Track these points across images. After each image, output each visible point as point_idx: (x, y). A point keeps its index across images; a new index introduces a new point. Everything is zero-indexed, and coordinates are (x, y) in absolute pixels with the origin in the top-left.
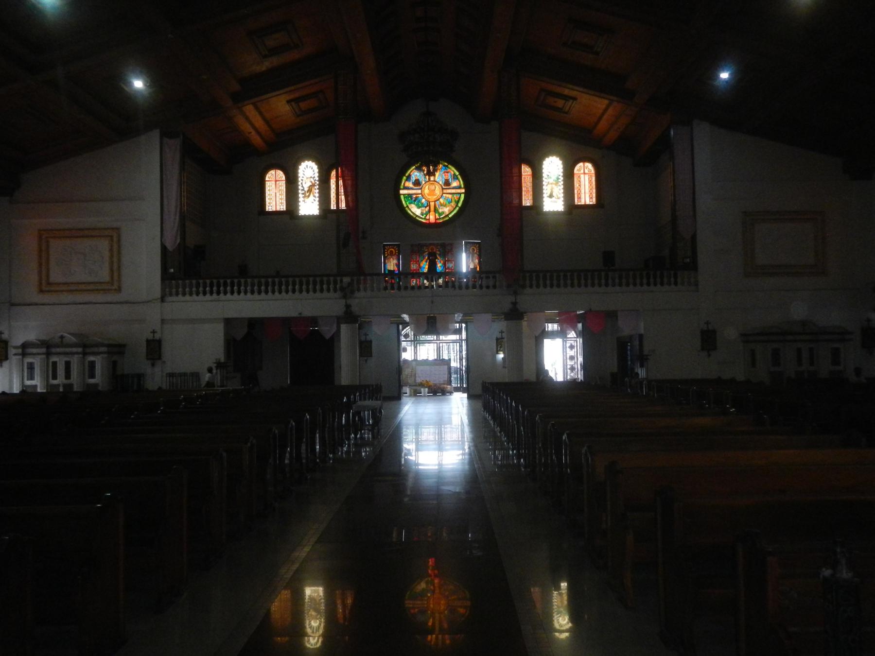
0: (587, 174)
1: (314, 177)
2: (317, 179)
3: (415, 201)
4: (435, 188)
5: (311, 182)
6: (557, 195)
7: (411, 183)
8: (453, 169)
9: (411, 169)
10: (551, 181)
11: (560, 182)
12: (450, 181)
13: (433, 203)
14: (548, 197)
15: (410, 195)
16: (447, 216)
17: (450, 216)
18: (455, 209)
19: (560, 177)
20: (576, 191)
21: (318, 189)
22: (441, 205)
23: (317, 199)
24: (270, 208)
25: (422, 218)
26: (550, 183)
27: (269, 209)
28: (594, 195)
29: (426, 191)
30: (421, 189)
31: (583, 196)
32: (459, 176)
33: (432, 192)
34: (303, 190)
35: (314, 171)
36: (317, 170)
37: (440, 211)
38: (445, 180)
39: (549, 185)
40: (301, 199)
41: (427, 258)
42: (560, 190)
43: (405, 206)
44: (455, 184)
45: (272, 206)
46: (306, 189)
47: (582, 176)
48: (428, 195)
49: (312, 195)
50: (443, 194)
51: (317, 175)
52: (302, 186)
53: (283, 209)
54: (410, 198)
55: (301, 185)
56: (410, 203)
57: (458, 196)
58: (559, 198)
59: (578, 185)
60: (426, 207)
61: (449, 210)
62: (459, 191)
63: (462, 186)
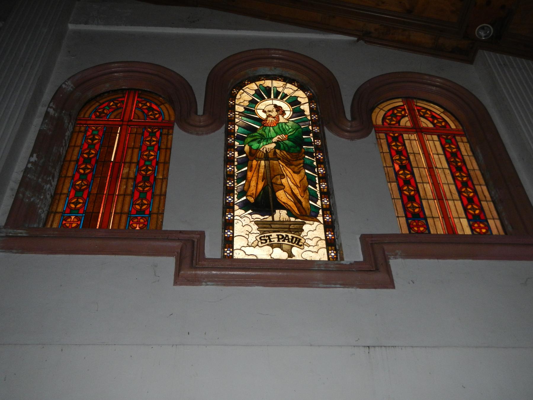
0: (428, 131)
6: (298, 202)
14: (245, 206)
26: (259, 154)
59: (397, 167)
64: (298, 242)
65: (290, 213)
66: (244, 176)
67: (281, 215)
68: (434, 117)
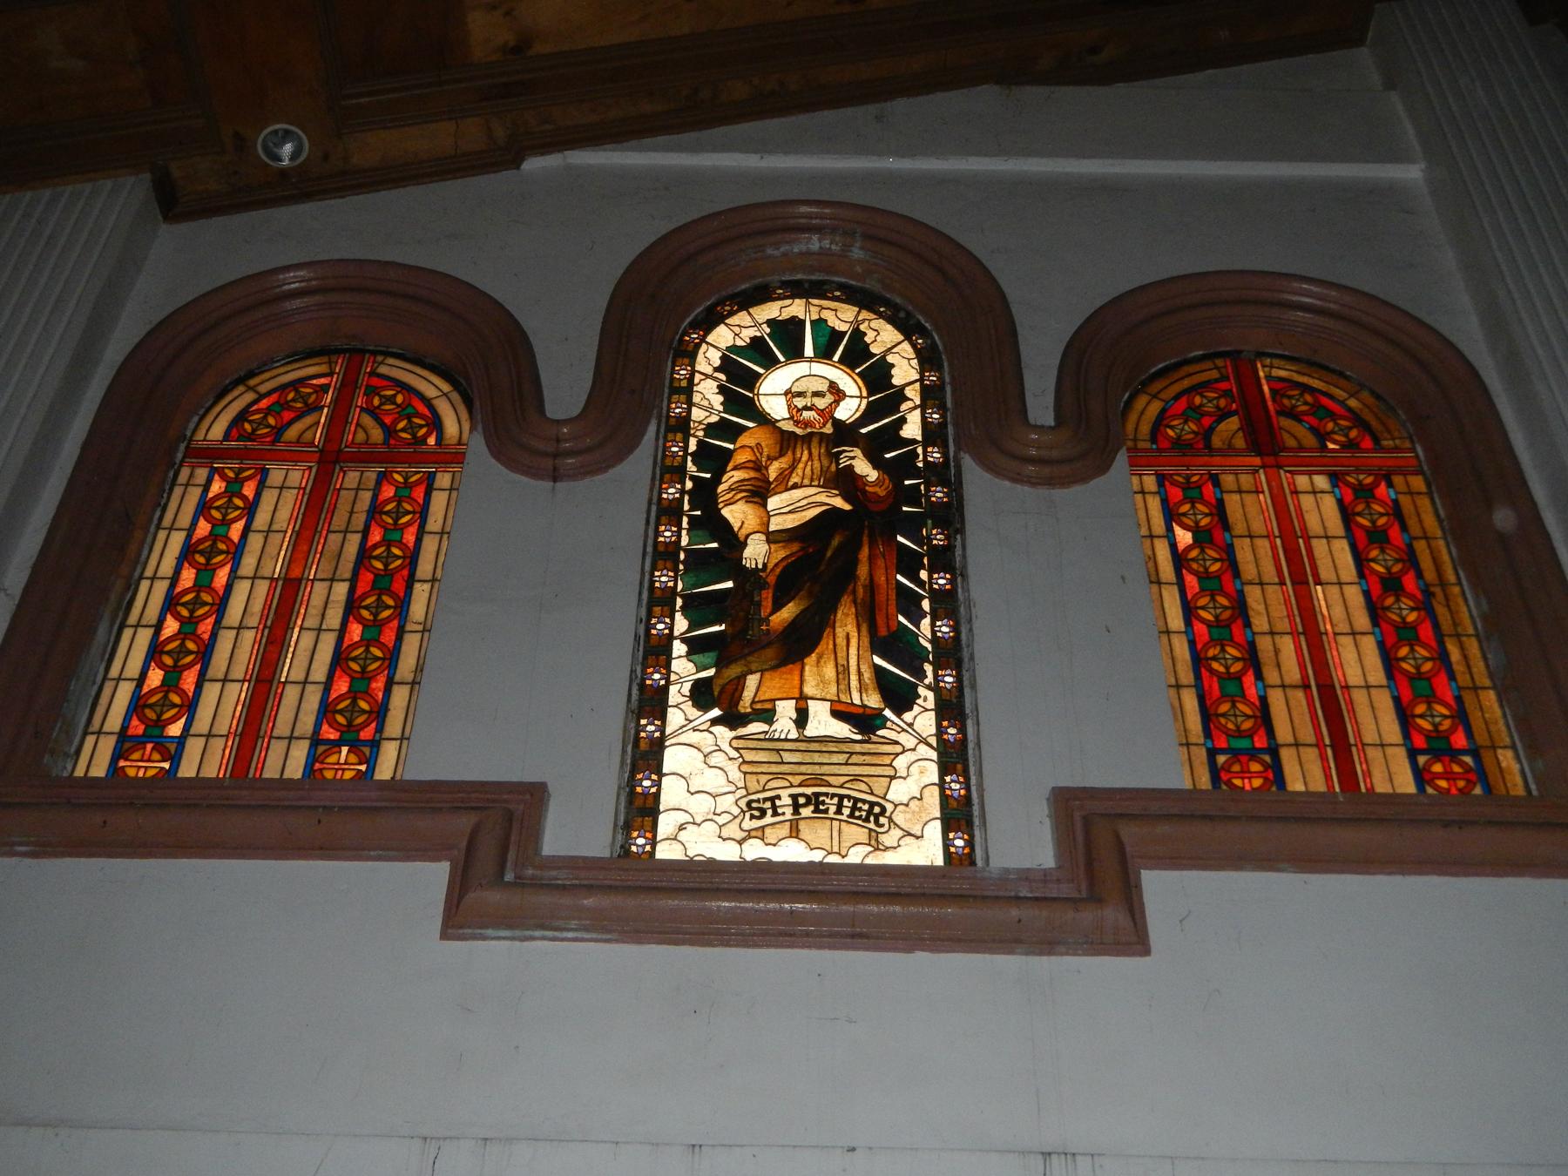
36: (904, 370)
49: (846, 626)
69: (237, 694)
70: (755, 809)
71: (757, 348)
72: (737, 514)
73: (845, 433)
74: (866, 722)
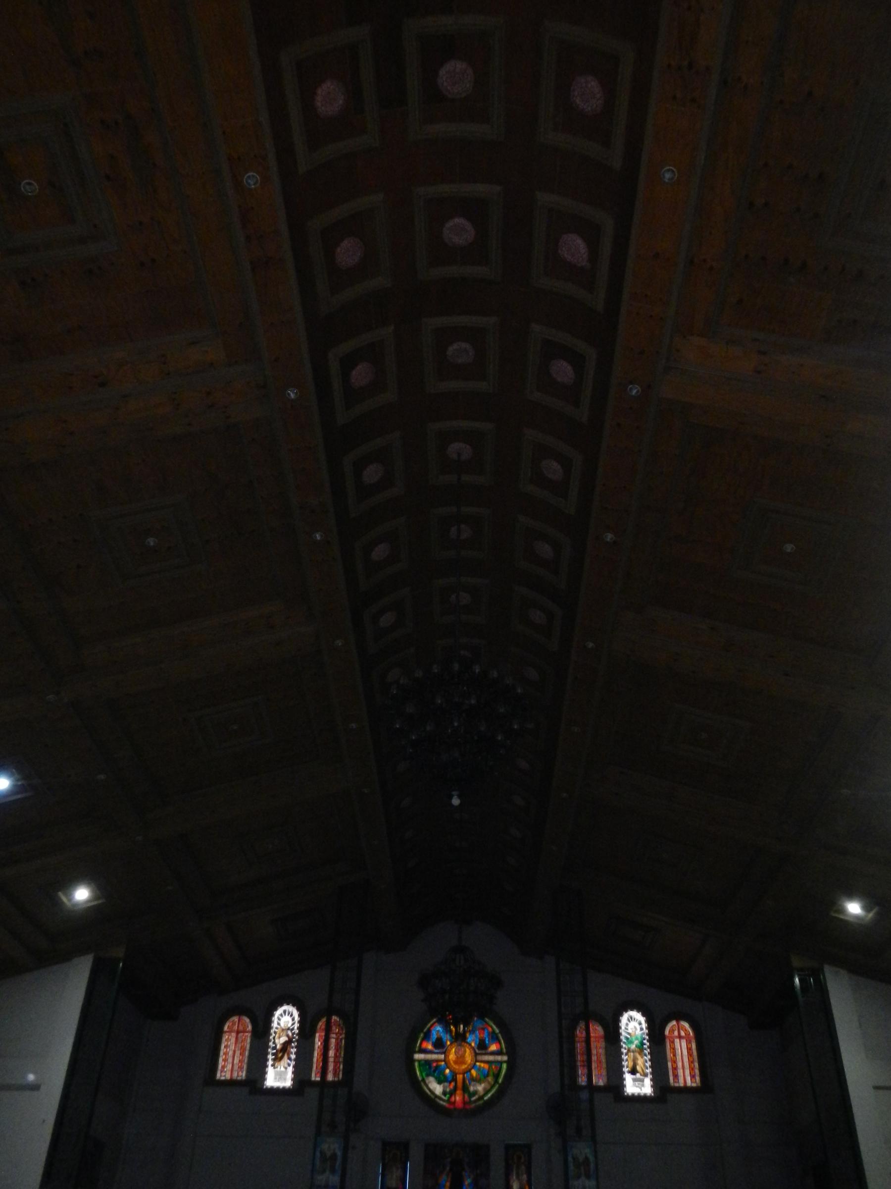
1: (293, 1029)
2: (297, 1031)
3: (434, 1071)
4: (465, 1051)
5: (288, 1036)
6: (643, 1071)
7: (431, 1042)
8: (491, 1024)
9: (432, 1023)
10: (633, 1047)
11: (646, 1049)
12: (487, 1042)
13: (461, 1076)
14: (629, 1072)
15: (428, 1063)
16: (481, 1098)
17: (486, 1098)
18: (492, 1087)
19: (645, 1041)
20: (670, 1064)
21: (296, 1047)
22: (473, 1079)
23: (293, 1063)
24: (223, 1074)
25: (443, 1100)
26: (631, 1050)
27: (221, 1076)
28: (697, 1072)
29: (452, 1056)
30: (444, 1053)
31: (680, 1072)
32: (500, 1035)
33: (460, 1060)
34: (274, 1048)
35: (293, 1019)
36: (297, 1018)
37: (472, 1089)
38: (480, 1040)
39: (629, 1054)
40: (270, 1063)
41: (448, 1168)
42: (646, 1062)
43: (420, 1079)
44: (493, 1048)
45: (226, 1072)
46: (278, 1047)
47: (677, 1041)
48: (456, 1062)
49: (286, 1057)
50: (477, 1061)
51: (296, 1025)
52: (274, 1043)
53: (242, 1076)
54: (427, 1067)
55: (273, 1040)
56: (428, 1075)
57: (499, 1066)
58: (646, 1075)
59: (672, 1055)
60: (450, 1083)
61: (484, 1089)
62: (499, 1058)
63: (504, 1050)
64: (643, 1085)
65: (641, 1075)
66: (627, 1060)
67: (638, 1075)
68: (686, 1030)
69: (231, 1065)
70: (275, 1078)
71: (281, 1015)
72: (277, 1041)
73: (289, 1029)
74: (286, 1068)
